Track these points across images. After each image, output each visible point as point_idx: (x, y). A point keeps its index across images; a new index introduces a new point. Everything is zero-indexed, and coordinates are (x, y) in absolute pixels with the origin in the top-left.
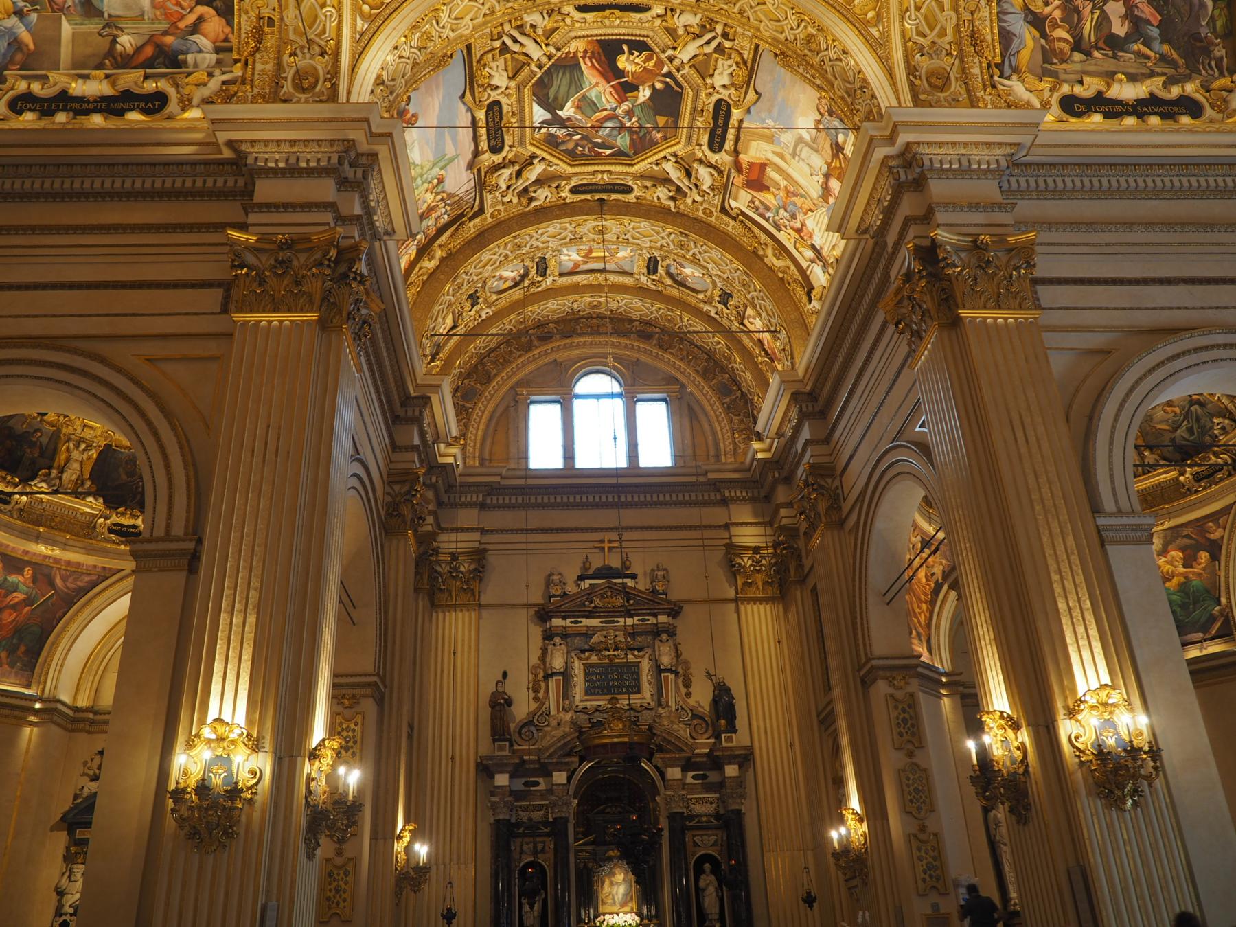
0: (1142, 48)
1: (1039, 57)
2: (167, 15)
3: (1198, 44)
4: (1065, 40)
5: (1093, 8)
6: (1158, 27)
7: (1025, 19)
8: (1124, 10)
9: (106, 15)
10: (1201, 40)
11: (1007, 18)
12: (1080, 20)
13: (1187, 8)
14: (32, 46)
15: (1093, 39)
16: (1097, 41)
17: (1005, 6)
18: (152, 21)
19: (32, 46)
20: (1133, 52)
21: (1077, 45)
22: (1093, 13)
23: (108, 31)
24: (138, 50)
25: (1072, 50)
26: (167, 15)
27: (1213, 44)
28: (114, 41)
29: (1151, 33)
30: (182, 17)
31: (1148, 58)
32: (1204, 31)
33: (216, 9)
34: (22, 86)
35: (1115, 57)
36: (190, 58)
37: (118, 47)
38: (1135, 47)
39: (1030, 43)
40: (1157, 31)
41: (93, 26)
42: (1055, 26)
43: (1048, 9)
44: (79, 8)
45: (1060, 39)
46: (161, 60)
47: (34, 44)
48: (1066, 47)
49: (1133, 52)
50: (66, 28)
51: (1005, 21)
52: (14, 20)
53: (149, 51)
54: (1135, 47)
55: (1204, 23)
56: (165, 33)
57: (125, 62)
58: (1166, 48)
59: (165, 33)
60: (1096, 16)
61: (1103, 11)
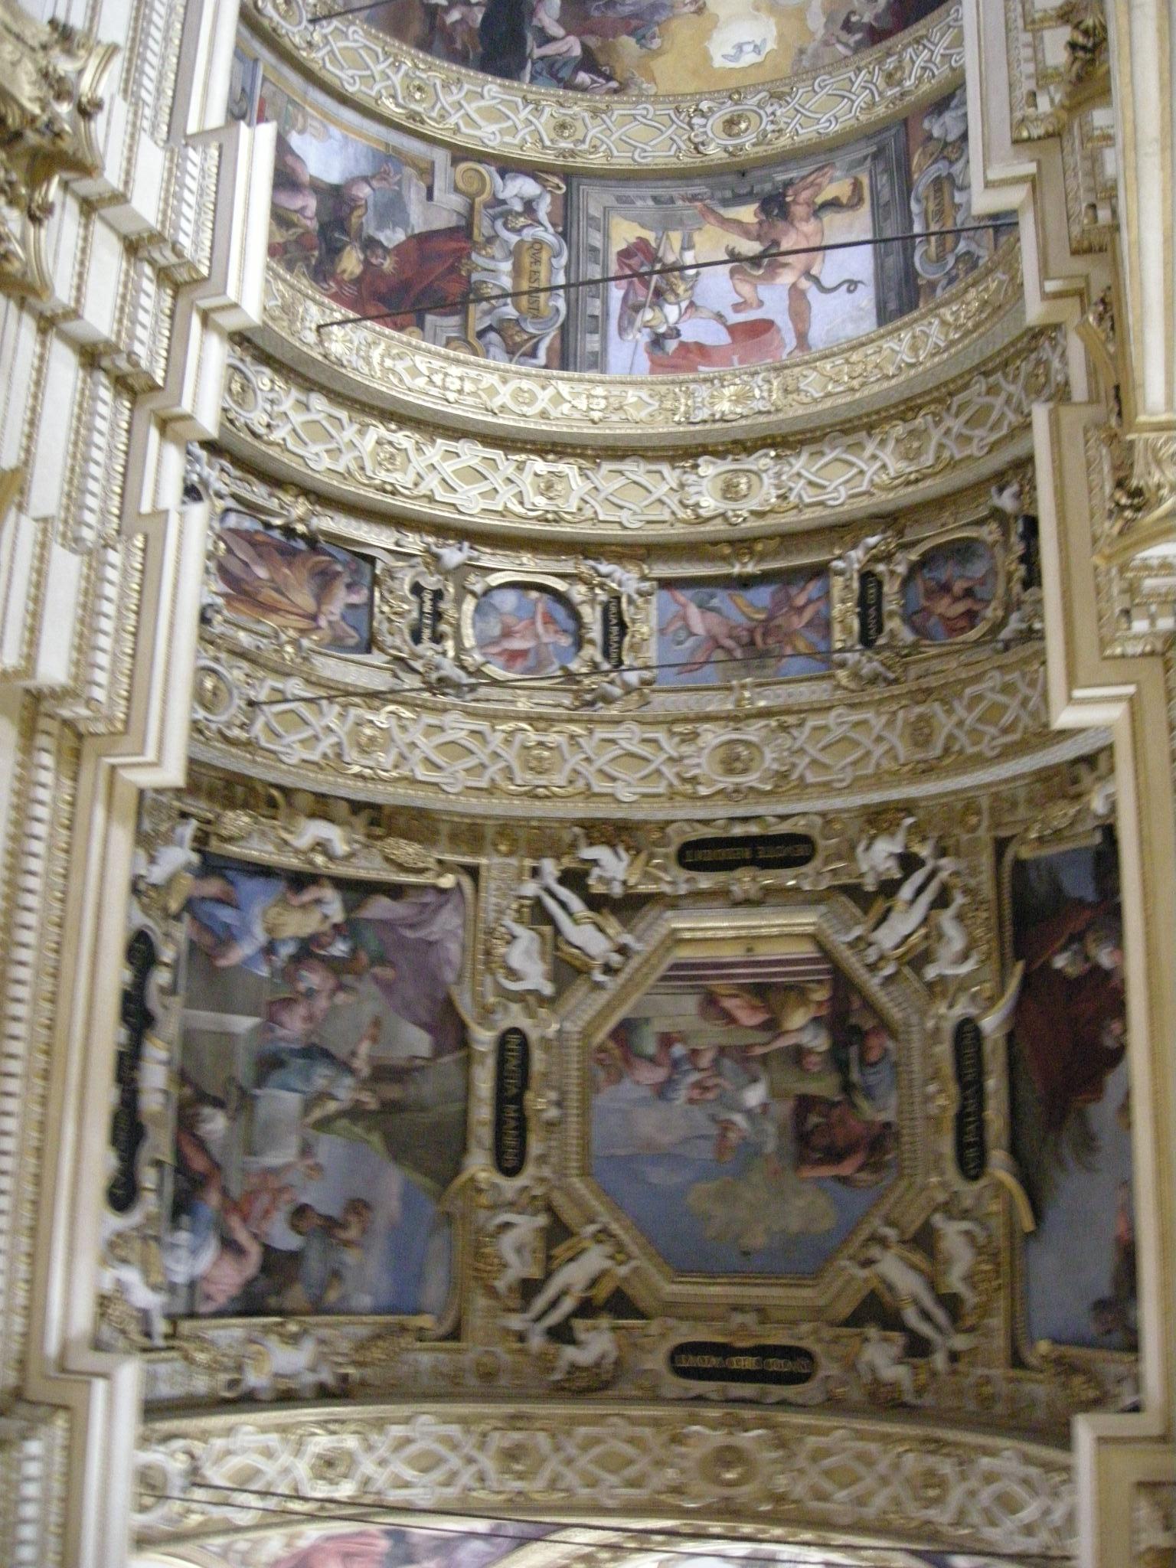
2: (251, 1195)
9: (258, 1092)
14: (222, 963)
18: (245, 1172)
19: (222, 963)
23: (234, 1093)
24: (201, 1145)
26: (251, 1195)
28: (219, 1104)
30: (245, 1219)
33: (255, 1279)
34: (167, 954)
36: (183, 1237)
37: (207, 1111)
41: (243, 1069)
44: (271, 1047)
46: (186, 1185)
47: (224, 969)
50: (243, 1024)
52: (261, 937)
53: (199, 1163)
56: (225, 1192)
57: (186, 1123)
59: (225, 1192)
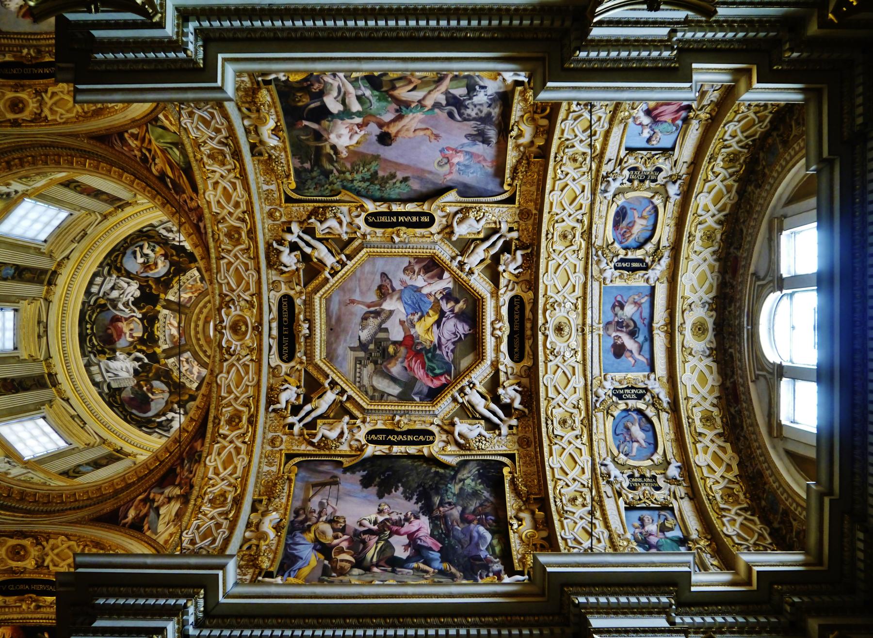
0: (422, 566)
1: (319, 572)
3: (478, 563)
4: (347, 561)
5: (379, 540)
6: (439, 552)
7: (314, 548)
8: (407, 541)
10: (481, 559)
11: (297, 547)
12: (365, 548)
13: (468, 539)
15: (375, 560)
16: (378, 561)
17: (297, 540)
20: (413, 569)
21: (360, 563)
22: (377, 543)
25: (352, 567)
27: (492, 562)
29: (431, 556)
31: (427, 572)
32: (484, 554)
35: (393, 571)
38: (415, 565)
39: (313, 562)
40: (439, 554)
42: (341, 551)
43: (336, 541)
45: (342, 561)
48: (347, 565)
49: (413, 569)
51: (295, 549)
54: (415, 565)
55: (483, 548)
58: (445, 566)
60: (380, 545)
61: (387, 541)
